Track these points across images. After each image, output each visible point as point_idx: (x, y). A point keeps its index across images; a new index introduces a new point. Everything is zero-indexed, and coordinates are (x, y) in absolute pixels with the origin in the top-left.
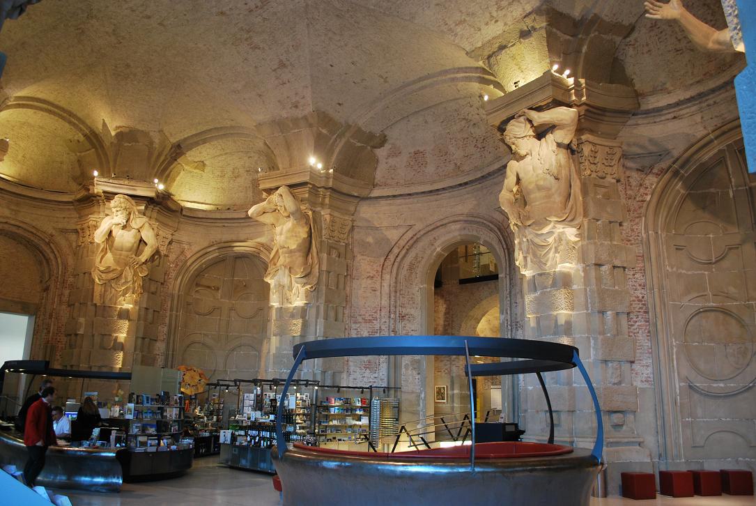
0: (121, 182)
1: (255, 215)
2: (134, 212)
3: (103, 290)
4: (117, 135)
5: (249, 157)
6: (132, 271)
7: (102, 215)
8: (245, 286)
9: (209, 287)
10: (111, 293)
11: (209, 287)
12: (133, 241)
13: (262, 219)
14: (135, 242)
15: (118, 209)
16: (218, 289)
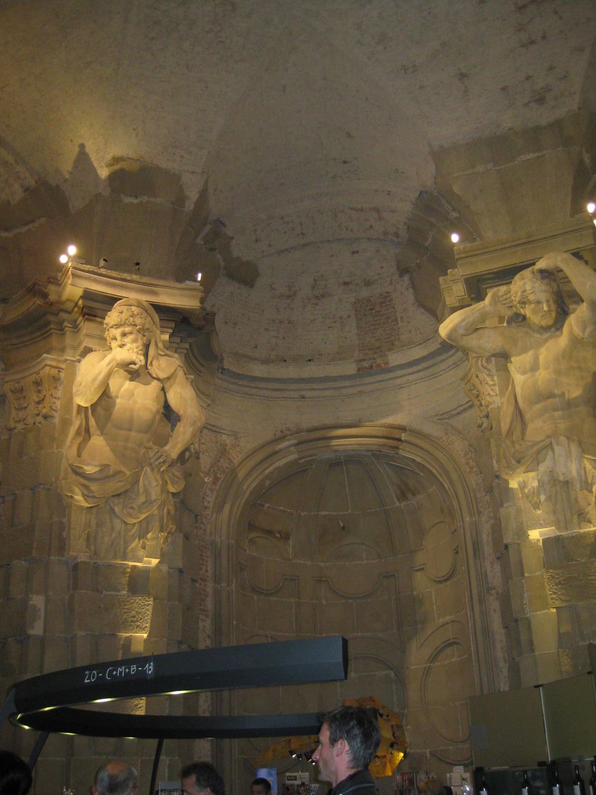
0: (125, 276)
1: (461, 331)
2: (156, 345)
3: (94, 522)
4: (112, 177)
5: (354, 253)
6: (159, 477)
7: (69, 356)
8: (343, 528)
9: (269, 532)
10: (113, 529)
11: (269, 532)
12: (154, 409)
13: (472, 341)
14: (157, 412)
15: (127, 329)
16: (286, 537)
